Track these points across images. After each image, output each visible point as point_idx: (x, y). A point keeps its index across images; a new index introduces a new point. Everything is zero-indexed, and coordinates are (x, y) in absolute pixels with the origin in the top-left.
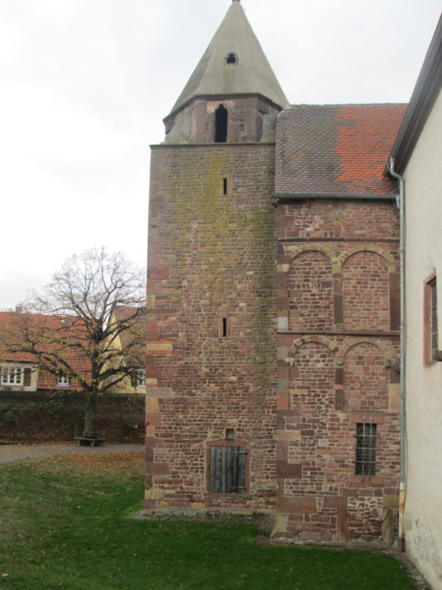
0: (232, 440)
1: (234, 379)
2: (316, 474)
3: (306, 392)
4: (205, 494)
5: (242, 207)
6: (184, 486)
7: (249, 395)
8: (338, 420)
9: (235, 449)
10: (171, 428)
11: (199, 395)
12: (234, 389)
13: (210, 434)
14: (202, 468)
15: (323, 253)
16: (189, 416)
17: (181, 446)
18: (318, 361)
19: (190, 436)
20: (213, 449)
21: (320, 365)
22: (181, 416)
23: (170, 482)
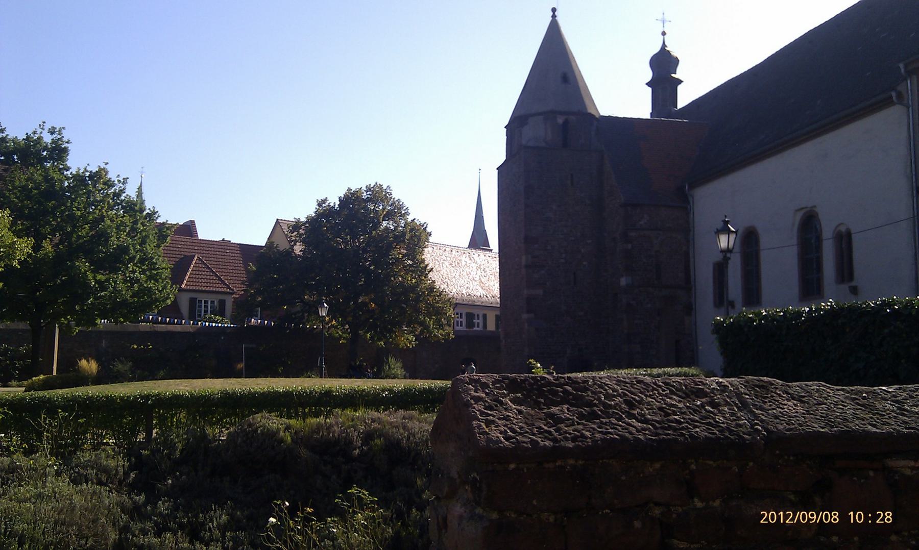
21: (649, 306)
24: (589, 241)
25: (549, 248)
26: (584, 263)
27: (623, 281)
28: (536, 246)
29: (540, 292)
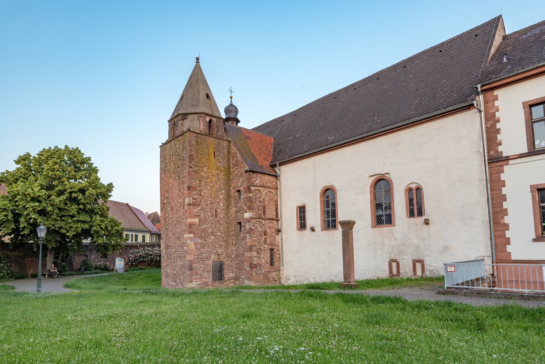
0: (220, 258)
1: (220, 234)
2: (260, 267)
3: (257, 239)
4: (211, 282)
5: (220, 164)
6: (204, 280)
7: (224, 240)
8: (265, 248)
9: (221, 262)
10: (199, 255)
11: (209, 241)
12: (220, 238)
13: (213, 257)
14: (210, 271)
15: (260, 191)
16: (205, 250)
17: (203, 263)
18: (259, 228)
19: (206, 258)
20: (214, 263)
21: (260, 229)
22: (203, 250)
23: (199, 279)
24: (223, 192)
25: (202, 194)
26: (221, 204)
27: (247, 215)
28: (195, 192)
29: (196, 220)
